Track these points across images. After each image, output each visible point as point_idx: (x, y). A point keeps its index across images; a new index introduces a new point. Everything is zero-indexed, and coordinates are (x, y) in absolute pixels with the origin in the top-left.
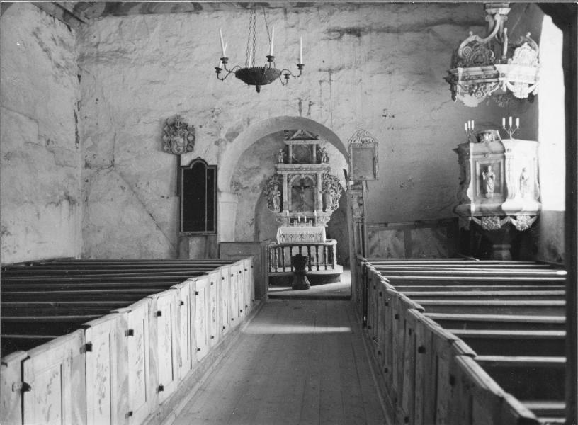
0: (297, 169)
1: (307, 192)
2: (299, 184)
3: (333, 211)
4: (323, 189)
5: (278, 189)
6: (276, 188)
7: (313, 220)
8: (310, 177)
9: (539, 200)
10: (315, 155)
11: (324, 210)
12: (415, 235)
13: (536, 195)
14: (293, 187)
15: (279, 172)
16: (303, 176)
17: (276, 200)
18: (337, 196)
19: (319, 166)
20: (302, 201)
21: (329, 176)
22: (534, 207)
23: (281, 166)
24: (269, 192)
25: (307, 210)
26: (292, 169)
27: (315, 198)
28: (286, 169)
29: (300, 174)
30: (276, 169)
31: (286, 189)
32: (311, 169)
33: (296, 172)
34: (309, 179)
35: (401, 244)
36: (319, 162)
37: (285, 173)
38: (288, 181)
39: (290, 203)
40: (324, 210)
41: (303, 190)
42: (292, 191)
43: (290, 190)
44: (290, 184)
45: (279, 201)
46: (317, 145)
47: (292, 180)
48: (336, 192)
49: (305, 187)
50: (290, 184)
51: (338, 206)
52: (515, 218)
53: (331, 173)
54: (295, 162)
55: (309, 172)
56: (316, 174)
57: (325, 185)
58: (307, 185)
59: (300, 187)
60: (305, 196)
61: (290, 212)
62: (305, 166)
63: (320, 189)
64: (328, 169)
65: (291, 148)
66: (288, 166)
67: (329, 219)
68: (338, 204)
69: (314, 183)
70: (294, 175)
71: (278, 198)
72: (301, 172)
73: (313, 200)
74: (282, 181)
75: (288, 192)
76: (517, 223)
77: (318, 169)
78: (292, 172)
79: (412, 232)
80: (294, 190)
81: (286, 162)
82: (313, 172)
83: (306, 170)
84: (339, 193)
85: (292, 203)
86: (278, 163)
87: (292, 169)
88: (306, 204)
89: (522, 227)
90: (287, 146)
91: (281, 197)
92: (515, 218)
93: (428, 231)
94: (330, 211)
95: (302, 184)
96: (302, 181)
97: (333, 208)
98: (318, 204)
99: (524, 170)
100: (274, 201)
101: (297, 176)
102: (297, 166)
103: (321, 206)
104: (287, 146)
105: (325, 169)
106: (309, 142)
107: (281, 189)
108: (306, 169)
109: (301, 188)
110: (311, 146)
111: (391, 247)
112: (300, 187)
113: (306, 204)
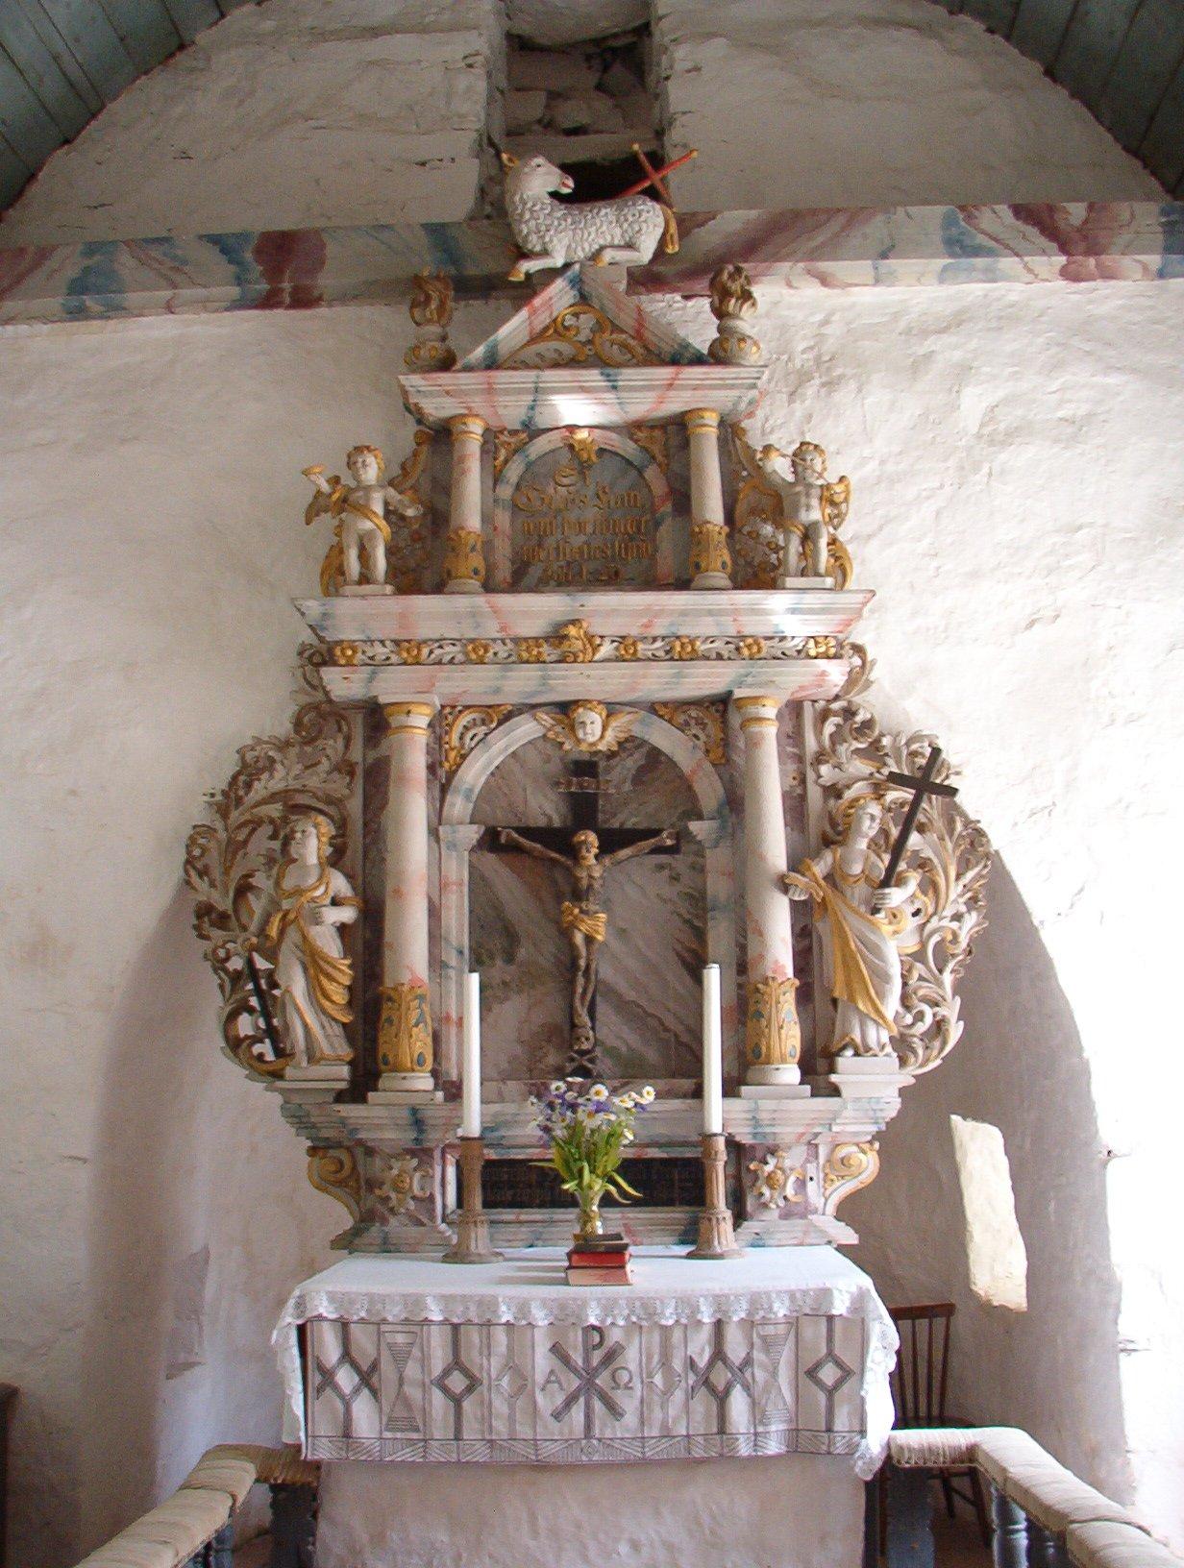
2: (545, 807)
3: (906, 1078)
5: (336, 858)
6: (312, 843)
8: (663, 736)
10: (712, 507)
14: (491, 841)
15: (343, 684)
16: (594, 732)
17: (314, 963)
18: (943, 923)
23: (370, 614)
24: (244, 889)
26: (475, 652)
28: (409, 651)
29: (565, 709)
30: (321, 655)
31: (428, 861)
32: (681, 651)
33: (521, 683)
34: (655, 757)
37: (417, 704)
38: (442, 779)
41: (592, 864)
42: (478, 882)
43: (457, 869)
45: (344, 972)
46: (730, 431)
47: (474, 773)
48: (930, 886)
49: (612, 842)
50: (458, 806)
51: (955, 1031)
53: (870, 704)
55: (658, 681)
56: (722, 703)
57: (821, 830)
58: (630, 819)
59: (560, 841)
65: (473, 446)
66: (432, 615)
67: (868, 1164)
68: (951, 1009)
69: (709, 790)
70: (501, 716)
71: (330, 946)
72: (569, 681)
74: (377, 781)
75: (439, 886)
78: (475, 683)
80: (490, 861)
82: (704, 680)
83: (626, 653)
84: (955, 894)
87: (475, 652)
88: (622, 1005)
90: (441, 436)
91: (368, 938)
94: (873, 1083)
95: (583, 810)
97: (902, 1046)
100: (296, 984)
101: (526, 729)
104: (441, 436)
106: (649, 394)
108: (627, 650)
109: (573, 852)
110: (678, 429)
112: (560, 841)
113: (622, 1005)
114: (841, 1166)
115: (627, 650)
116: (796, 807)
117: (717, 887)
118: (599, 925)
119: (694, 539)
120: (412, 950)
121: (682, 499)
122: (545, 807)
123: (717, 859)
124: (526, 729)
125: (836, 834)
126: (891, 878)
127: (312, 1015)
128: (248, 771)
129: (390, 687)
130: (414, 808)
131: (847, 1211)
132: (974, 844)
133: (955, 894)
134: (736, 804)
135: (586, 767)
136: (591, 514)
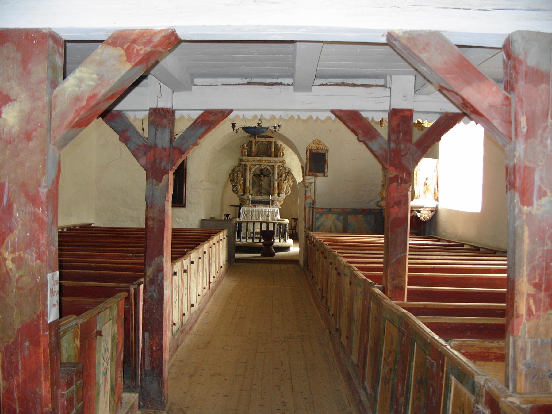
0: (258, 161)
1: (266, 178)
2: (259, 173)
4: (278, 179)
5: (242, 176)
7: (267, 203)
9: (437, 200)
10: (273, 150)
11: (278, 195)
12: (351, 219)
13: (435, 196)
14: (254, 175)
15: (243, 163)
16: (263, 167)
17: (240, 185)
19: (276, 159)
20: (260, 186)
21: (285, 168)
22: (433, 204)
23: (245, 158)
25: (264, 194)
27: (272, 185)
28: (248, 161)
29: (260, 165)
31: (249, 177)
32: (270, 162)
35: (340, 225)
36: (276, 156)
38: (250, 170)
39: (251, 188)
40: (278, 195)
41: (262, 178)
42: (253, 179)
43: (251, 177)
44: (252, 172)
46: (275, 142)
47: (253, 170)
49: (264, 176)
50: (252, 172)
52: (419, 212)
54: (256, 155)
55: (268, 164)
59: (260, 176)
60: (264, 182)
61: (251, 195)
62: (264, 158)
63: (276, 176)
64: (283, 162)
66: (250, 158)
67: (283, 202)
69: (272, 172)
71: (242, 184)
72: (261, 163)
73: (270, 186)
74: (245, 170)
76: (421, 216)
77: (275, 162)
78: (254, 163)
79: (349, 216)
80: (255, 178)
81: (249, 155)
83: (265, 162)
84: (291, 181)
85: (253, 188)
86: (242, 156)
87: (254, 161)
89: (424, 218)
90: (251, 142)
91: (244, 183)
92: (419, 212)
93: (360, 217)
95: (262, 173)
96: (262, 170)
98: (274, 189)
99: (427, 179)
101: (257, 166)
102: (258, 158)
103: (276, 191)
104: (251, 142)
105: (280, 162)
106: (268, 140)
107: (244, 176)
108: (265, 161)
110: (271, 142)
111: (333, 226)
114: (280, 202)
115: (265, 161)
116: (278, 174)
117: (272, 180)
118: (262, 183)
119: (271, 152)
120: (248, 184)
121: (271, 148)
122: (259, 173)
123: (272, 178)
124: (257, 166)
125: (281, 176)
126: (285, 180)
127: (240, 189)
128: (234, 169)
129: (247, 163)
130: (248, 173)
131: (280, 206)
132: (293, 177)
133: (291, 181)
134: (274, 173)
135: (262, 170)
136: (263, 149)
